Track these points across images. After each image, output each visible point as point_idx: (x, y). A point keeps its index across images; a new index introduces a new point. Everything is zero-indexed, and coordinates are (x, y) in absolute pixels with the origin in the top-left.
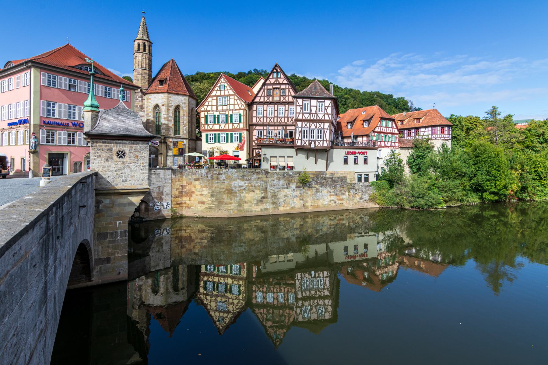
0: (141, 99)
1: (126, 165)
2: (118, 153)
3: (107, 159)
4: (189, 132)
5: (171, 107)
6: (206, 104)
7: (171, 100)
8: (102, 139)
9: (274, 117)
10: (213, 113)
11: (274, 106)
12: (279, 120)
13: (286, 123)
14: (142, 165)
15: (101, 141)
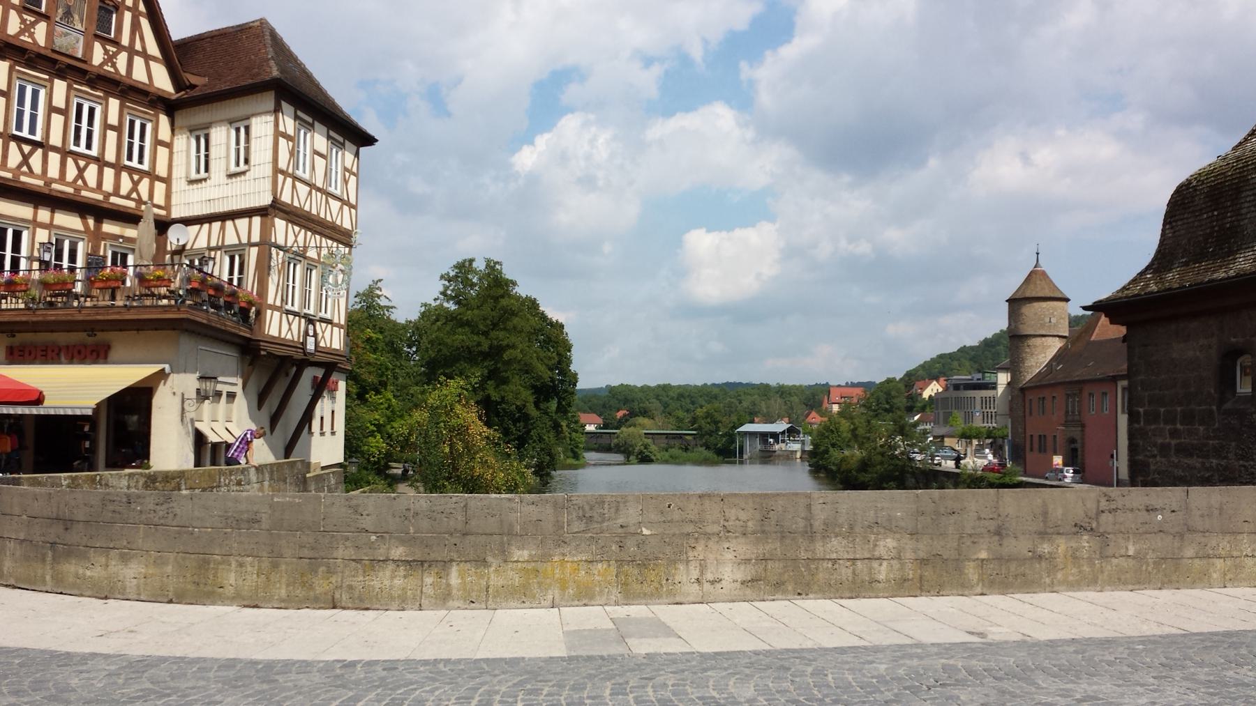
12: (71, 172)
13: (107, 195)
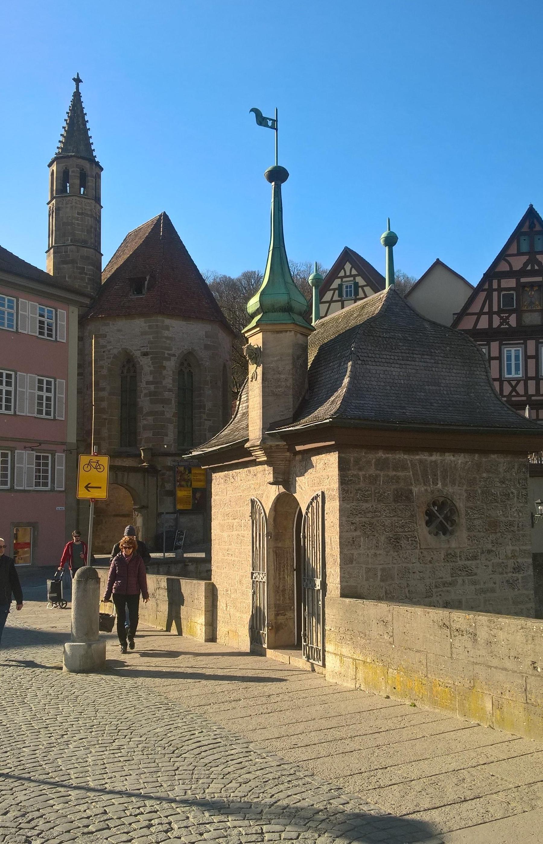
1: (460, 563)
2: (428, 513)
3: (397, 539)
5: (168, 359)
7: (167, 338)
8: (375, 448)
9: (527, 379)
11: (525, 344)
14: (511, 563)
15: (374, 456)
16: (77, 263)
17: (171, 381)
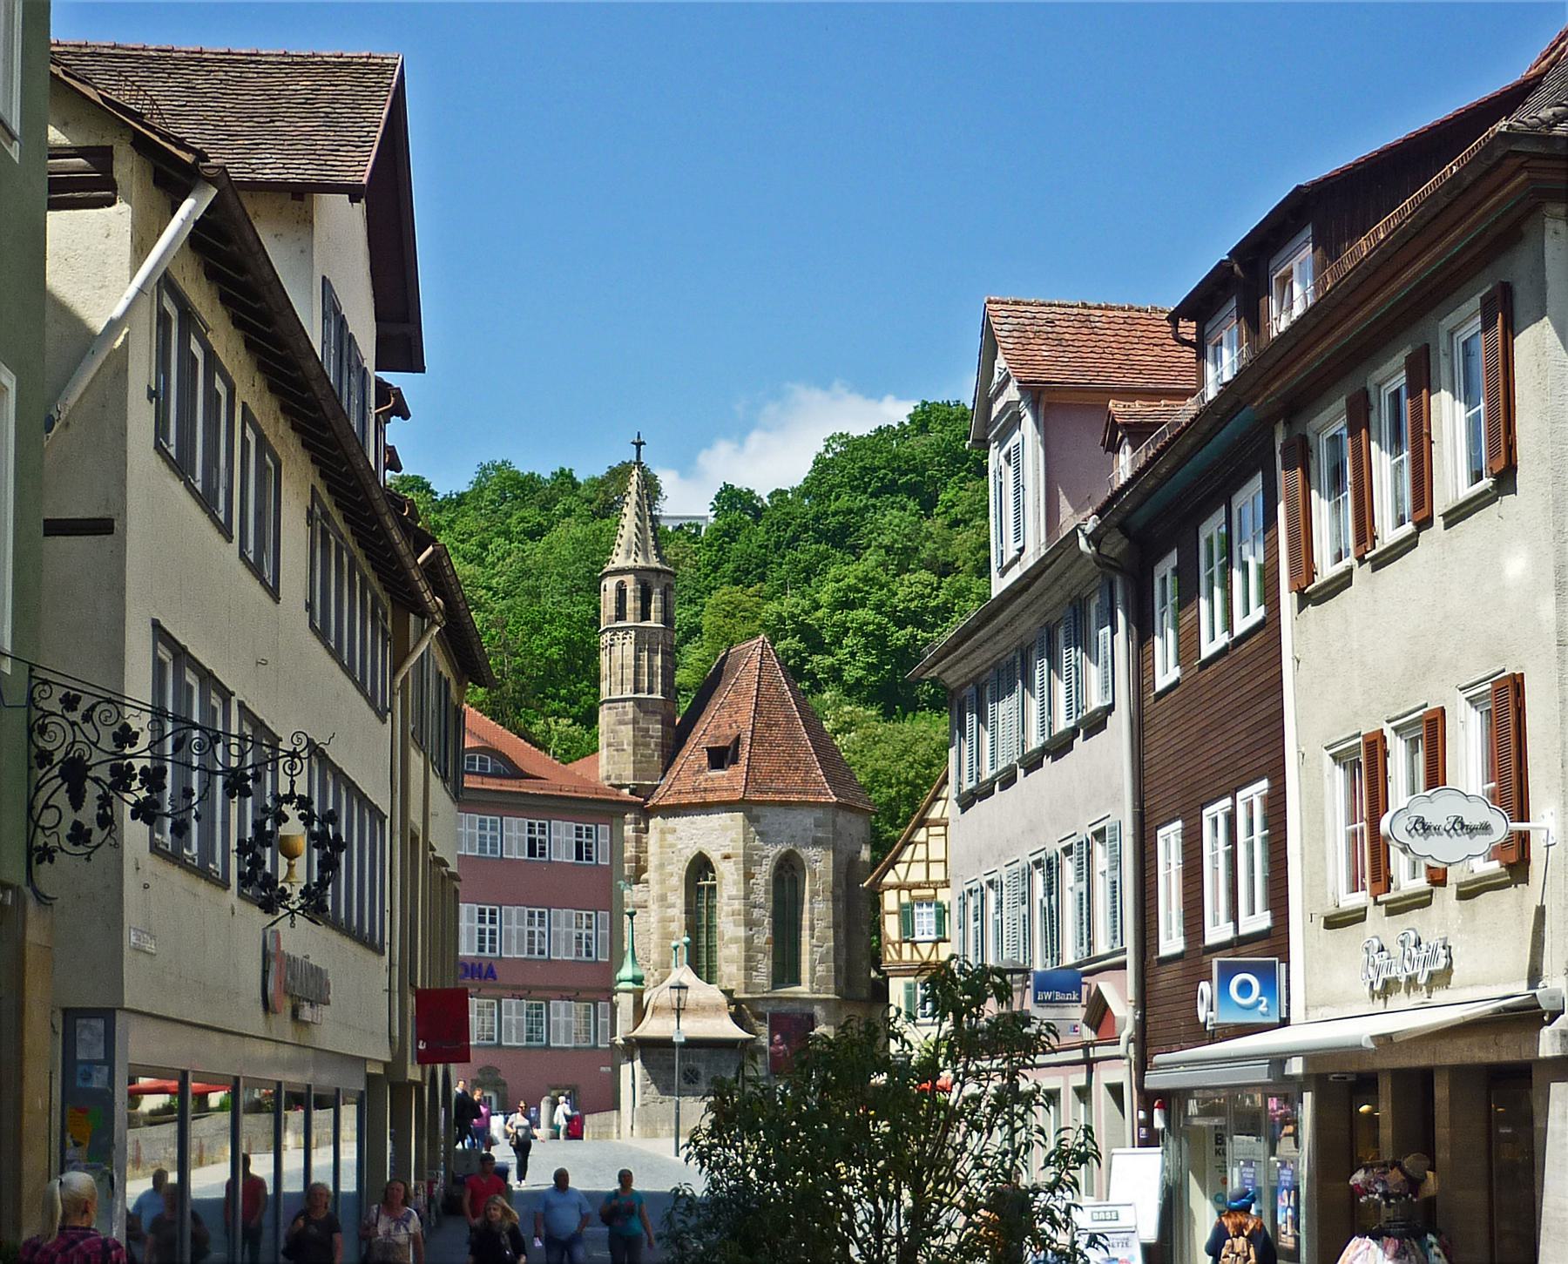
0: (636, 830)
2: (685, 1074)
4: (837, 970)
6: (906, 856)
10: (932, 892)
16: (638, 723)
17: (762, 894)
